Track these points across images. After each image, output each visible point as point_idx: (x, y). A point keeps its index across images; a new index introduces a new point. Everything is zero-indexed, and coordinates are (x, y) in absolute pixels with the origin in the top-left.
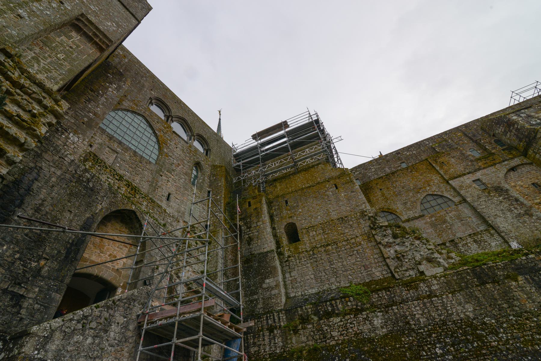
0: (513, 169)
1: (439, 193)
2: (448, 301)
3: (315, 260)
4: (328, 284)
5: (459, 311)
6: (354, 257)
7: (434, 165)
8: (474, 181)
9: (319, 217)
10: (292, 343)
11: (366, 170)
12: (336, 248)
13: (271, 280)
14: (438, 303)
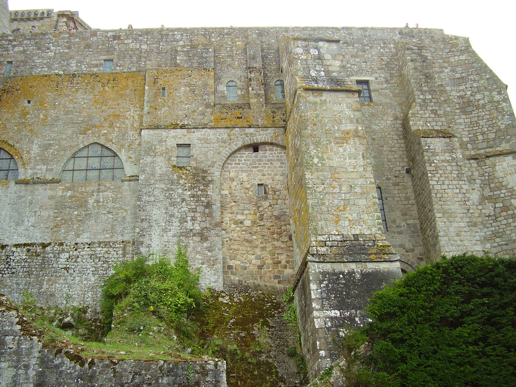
0: (256, 148)
1: (114, 148)
7: (147, 88)
8: (179, 145)
11: (39, 49)
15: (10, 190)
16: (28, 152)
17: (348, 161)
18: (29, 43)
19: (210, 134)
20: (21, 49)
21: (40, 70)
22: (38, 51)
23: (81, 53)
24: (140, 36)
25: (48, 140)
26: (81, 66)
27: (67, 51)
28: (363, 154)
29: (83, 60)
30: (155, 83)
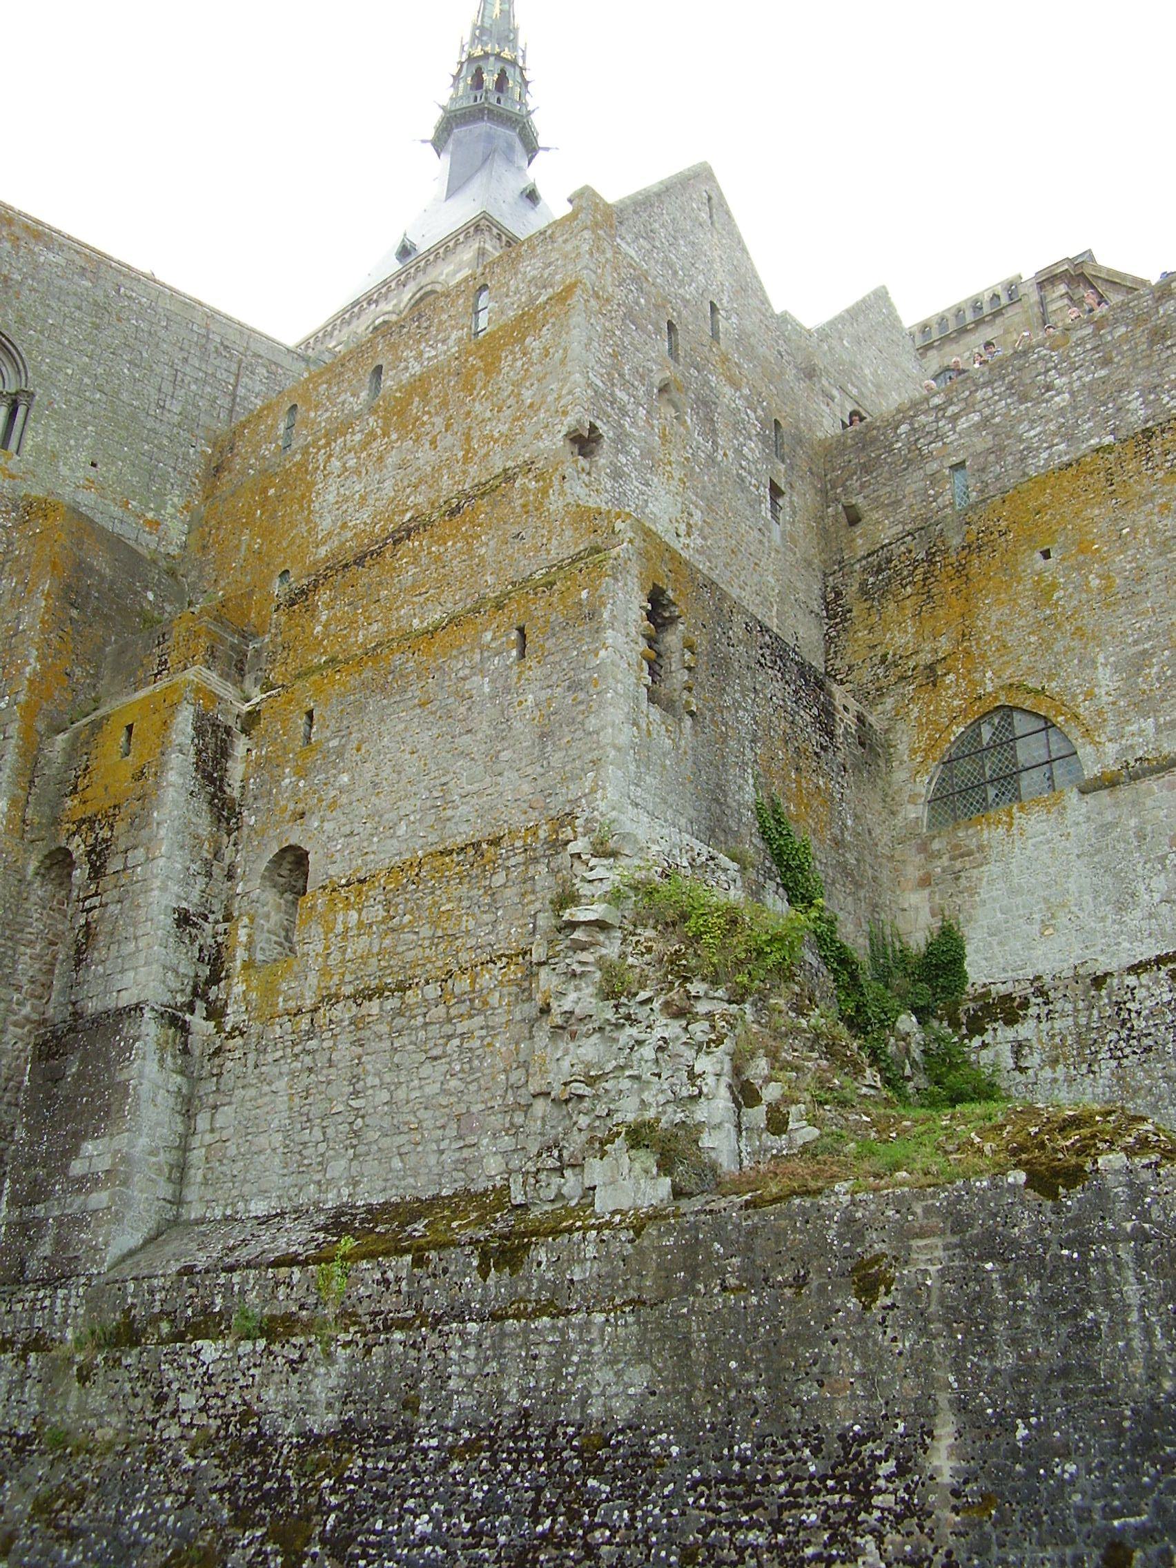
2: (582, 1341)
3: (308, 1060)
4: (319, 1183)
5: (595, 1390)
6: (441, 1066)
9: (402, 830)
10: (64, 1407)
11: (1023, 399)
12: (399, 1013)
13: (102, 1144)
14: (545, 1342)
15: (1071, 816)
16: (1090, 695)
18: (990, 394)
20: (976, 418)
21: (1045, 455)
22: (1022, 407)
23: (1146, 362)
25: (1136, 643)
26: (1158, 399)
27: (1103, 373)
29: (1157, 381)
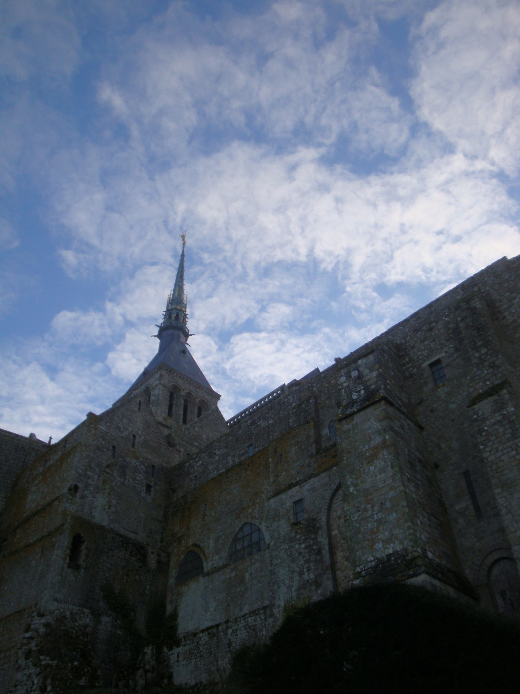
16: (208, 548)
17: (379, 477)
19: (315, 482)
20: (201, 462)
24: (267, 413)
28: (391, 463)
30: (275, 452)
